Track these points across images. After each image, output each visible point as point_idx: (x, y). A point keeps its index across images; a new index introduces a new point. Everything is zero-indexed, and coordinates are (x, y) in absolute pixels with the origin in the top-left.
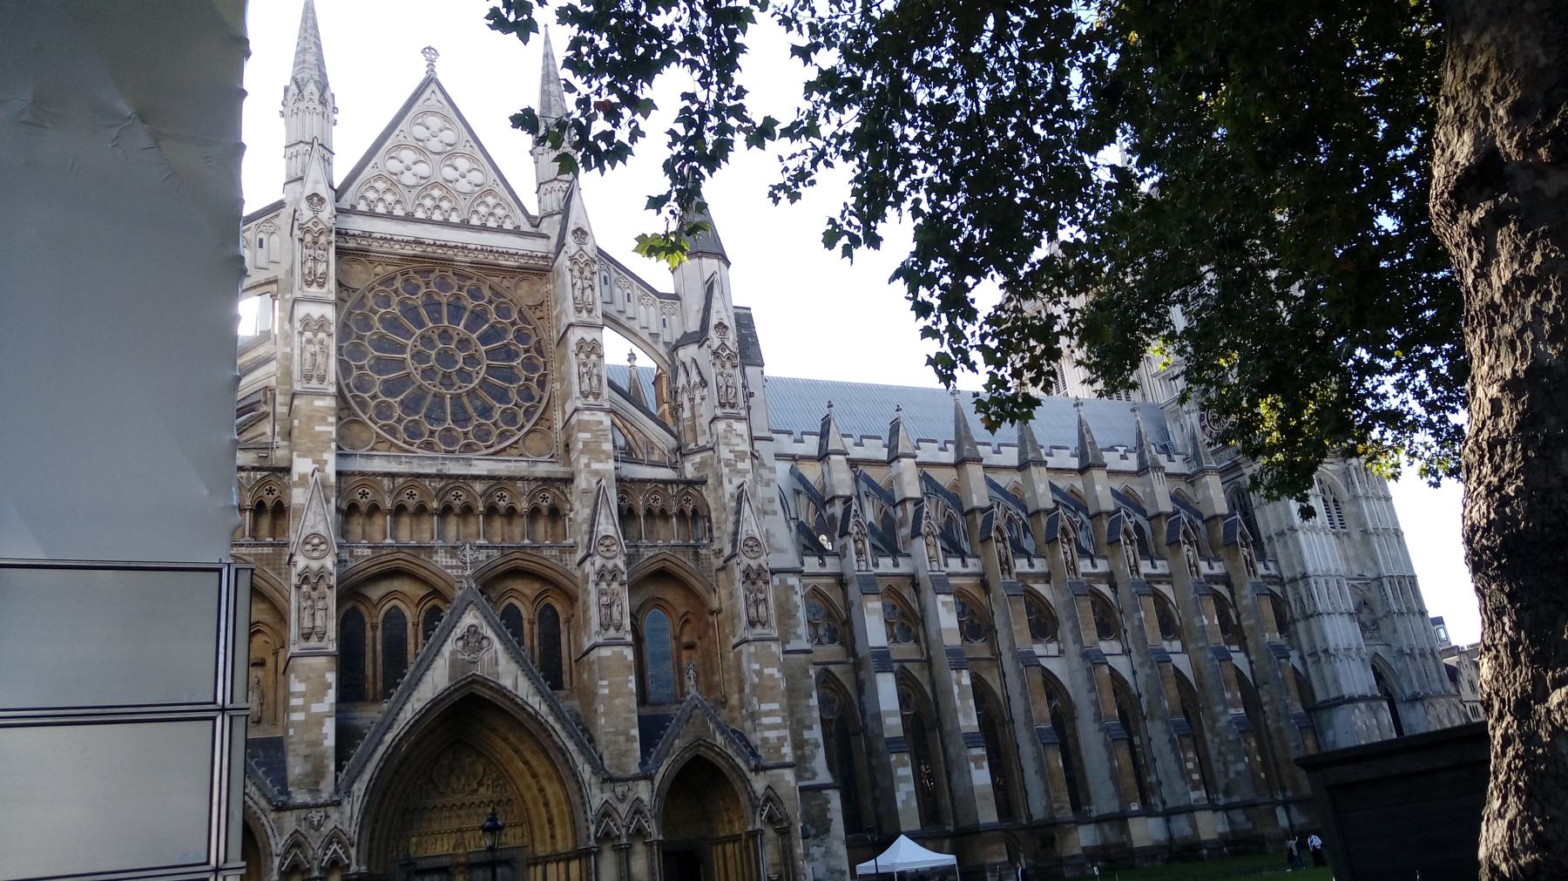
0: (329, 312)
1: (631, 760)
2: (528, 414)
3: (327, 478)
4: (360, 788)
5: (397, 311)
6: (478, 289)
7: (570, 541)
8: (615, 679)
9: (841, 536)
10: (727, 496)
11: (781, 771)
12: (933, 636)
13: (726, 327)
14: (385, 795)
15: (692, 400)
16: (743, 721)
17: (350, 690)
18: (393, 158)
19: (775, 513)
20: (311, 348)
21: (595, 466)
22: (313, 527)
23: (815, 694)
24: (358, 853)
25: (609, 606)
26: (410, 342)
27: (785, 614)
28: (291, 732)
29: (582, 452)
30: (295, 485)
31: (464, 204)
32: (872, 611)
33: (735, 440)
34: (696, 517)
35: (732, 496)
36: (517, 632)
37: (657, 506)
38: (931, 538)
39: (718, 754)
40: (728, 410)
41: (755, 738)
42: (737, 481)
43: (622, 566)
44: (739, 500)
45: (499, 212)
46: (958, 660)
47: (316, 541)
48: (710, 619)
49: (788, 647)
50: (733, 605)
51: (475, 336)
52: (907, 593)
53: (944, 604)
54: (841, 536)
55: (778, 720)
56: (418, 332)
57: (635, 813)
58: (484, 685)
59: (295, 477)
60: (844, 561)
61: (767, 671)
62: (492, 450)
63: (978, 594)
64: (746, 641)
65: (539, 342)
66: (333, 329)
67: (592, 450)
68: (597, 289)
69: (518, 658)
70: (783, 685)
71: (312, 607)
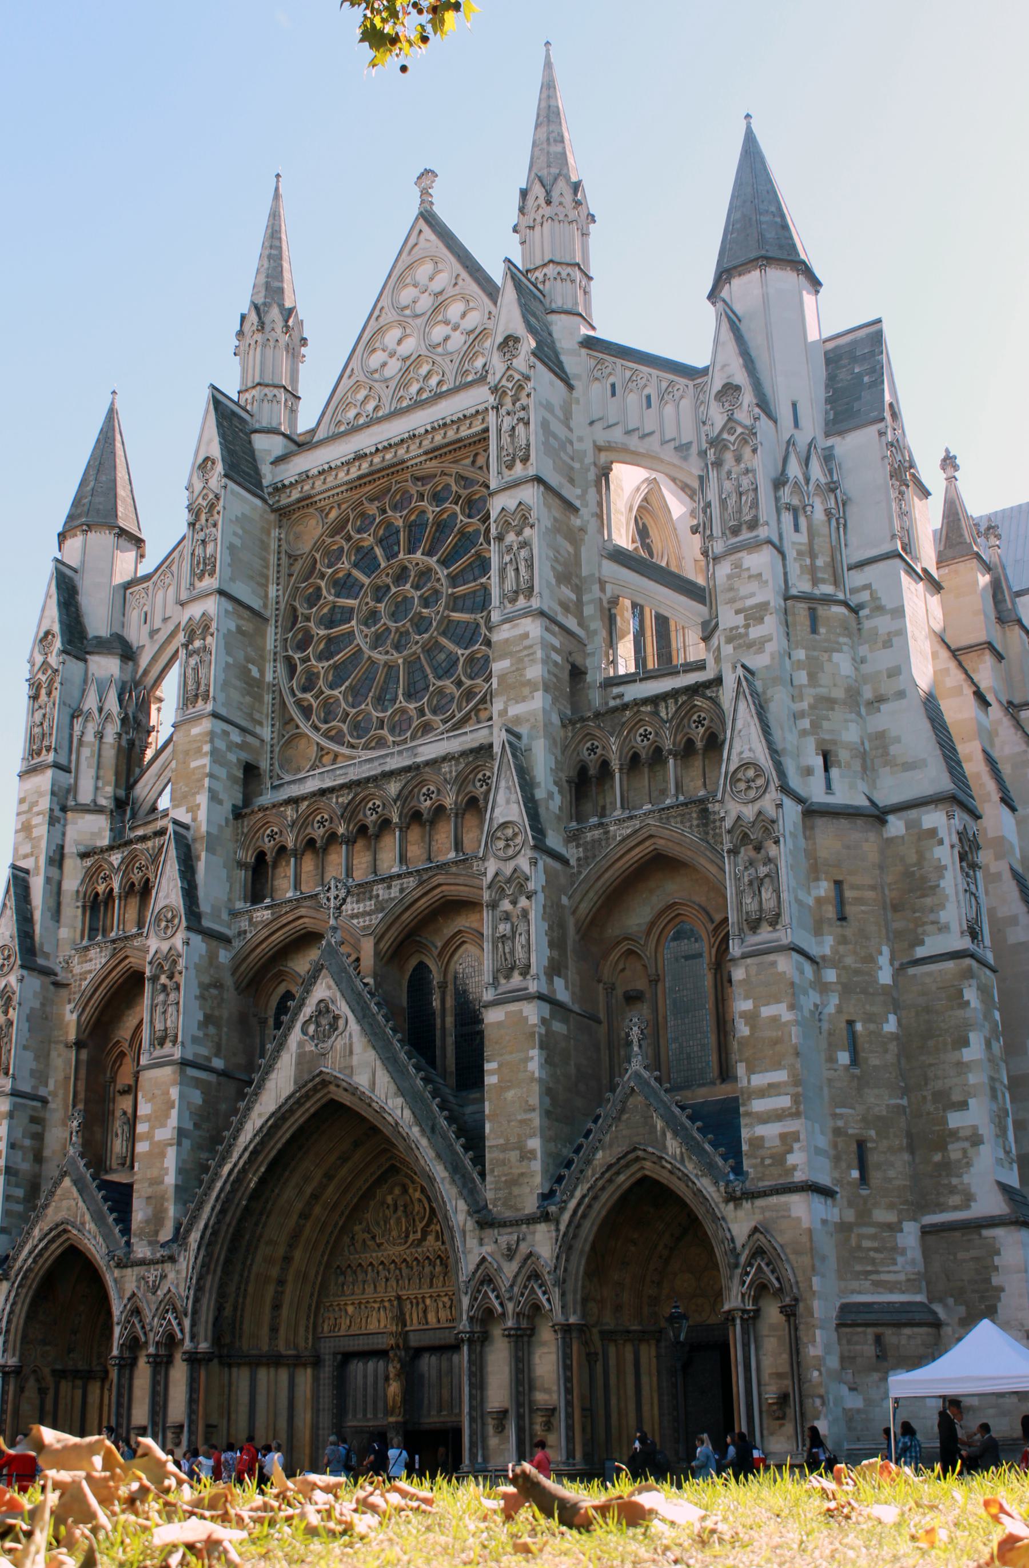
1: (527, 1190)
4: (194, 1237)
8: (508, 1058)
11: (783, 1199)
13: (738, 388)
14: (291, 1246)
18: (374, 350)
20: (192, 662)
21: (514, 710)
22: (167, 896)
24: (193, 1324)
28: (136, 1165)
31: (450, 370)
33: (743, 592)
37: (641, 745)
39: (671, 1172)
40: (745, 535)
47: (170, 915)
49: (921, 952)
55: (784, 1102)
56: (366, 581)
57: (529, 1279)
61: (766, 1011)
71: (165, 1003)
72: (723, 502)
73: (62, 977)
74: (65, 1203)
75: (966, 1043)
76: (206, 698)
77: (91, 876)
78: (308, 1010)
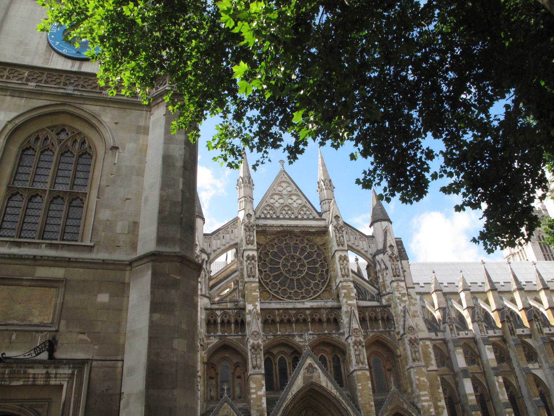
0: (255, 253)
2: (323, 284)
3: (257, 311)
5: (276, 251)
6: (303, 240)
7: (341, 331)
9: (443, 323)
10: (399, 312)
12: (485, 362)
13: (393, 246)
15: (383, 275)
16: (414, 399)
17: (270, 387)
19: (418, 316)
21: (349, 302)
23: (441, 387)
25: (359, 355)
26: (281, 261)
27: (426, 356)
28: (252, 401)
29: (344, 297)
30: (248, 314)
32: (459, 353)
33: (400, 289)
34: (388, 320)
35: (402, 311)
36: (326, 366)
38: (480, 322)
40: (397, 278)
41: (419, 405)
42: (403, 305)
43: (362, 340)
44: (404, 312)
45: (308, 213)
46: (497, 372)
47: (255, 334)
48: (397, 359)
49: (429, 369)
50: (406, 353)
51: (302, 257)
52: (472, 345)
53: (488, 349)
54: (443, 323)
55: (428, 398)
58: (316, 385)
59: (247, 311)
60: (445, 333)
61: (422, 379)
62: (311, 298)
63: (501, 344)
64: (412, 367)
65: (325, 257)
66: (256, 259)
67: (347, 296)
68: (345, 237)
69: (326, 375)
70: (428, 384)
71: (256, 357)
72: (393, 270)
73: (202, 343)
74: (226, 410)
75: (439, 388)
76: (254, 277)
77: (208, 316)
78: (306, 365)
